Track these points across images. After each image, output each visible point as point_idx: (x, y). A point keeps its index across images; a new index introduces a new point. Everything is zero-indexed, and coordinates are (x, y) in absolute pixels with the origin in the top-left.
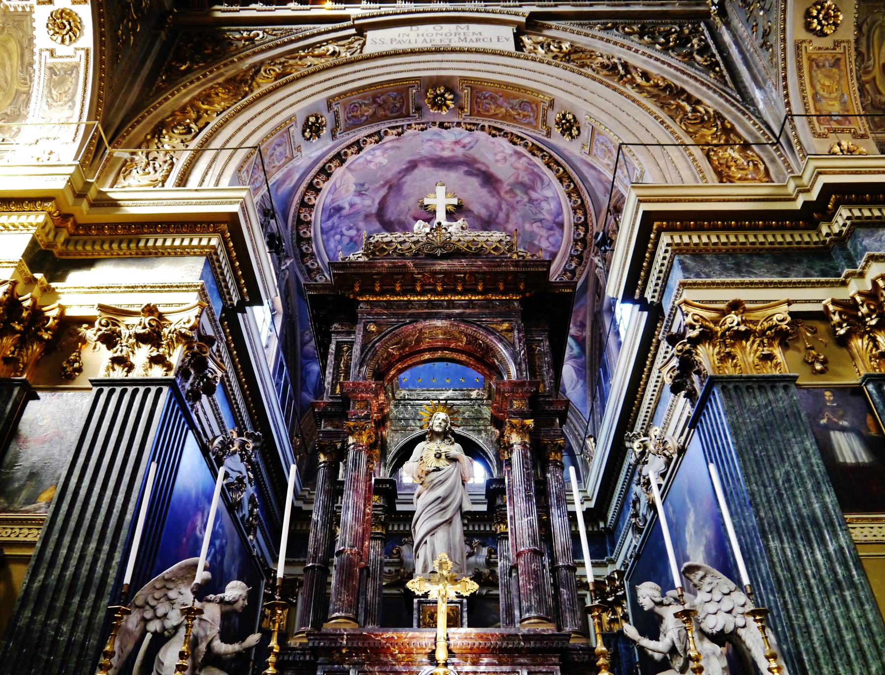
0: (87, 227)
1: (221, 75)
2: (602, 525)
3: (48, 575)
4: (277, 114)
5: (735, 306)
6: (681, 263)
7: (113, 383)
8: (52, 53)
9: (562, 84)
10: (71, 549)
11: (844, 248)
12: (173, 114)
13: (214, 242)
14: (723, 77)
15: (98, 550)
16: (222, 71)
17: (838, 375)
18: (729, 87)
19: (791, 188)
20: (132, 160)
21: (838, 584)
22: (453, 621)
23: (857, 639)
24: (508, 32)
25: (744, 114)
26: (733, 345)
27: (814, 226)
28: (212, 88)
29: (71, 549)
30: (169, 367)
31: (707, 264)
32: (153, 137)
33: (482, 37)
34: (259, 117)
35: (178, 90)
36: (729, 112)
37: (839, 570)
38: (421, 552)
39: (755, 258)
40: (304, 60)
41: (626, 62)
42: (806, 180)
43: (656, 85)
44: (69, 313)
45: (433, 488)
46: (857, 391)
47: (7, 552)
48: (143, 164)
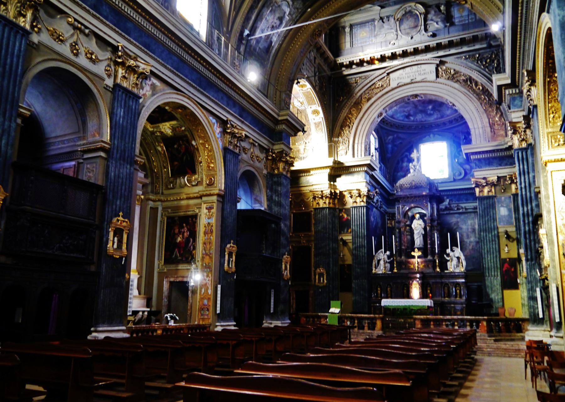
0: (337, 168)
1: (352, 102)
5: (484, 178)
7: (355, 207)
8: (314, 119)
17: (507, 192)
21: (492, 241)
24: (433, 67)
30: (364, 202)
31: (481, 163)
33: (425, 72)
37: (493, 238)
41: (471, 77)
43: (479, 88)
44: (341, 190)
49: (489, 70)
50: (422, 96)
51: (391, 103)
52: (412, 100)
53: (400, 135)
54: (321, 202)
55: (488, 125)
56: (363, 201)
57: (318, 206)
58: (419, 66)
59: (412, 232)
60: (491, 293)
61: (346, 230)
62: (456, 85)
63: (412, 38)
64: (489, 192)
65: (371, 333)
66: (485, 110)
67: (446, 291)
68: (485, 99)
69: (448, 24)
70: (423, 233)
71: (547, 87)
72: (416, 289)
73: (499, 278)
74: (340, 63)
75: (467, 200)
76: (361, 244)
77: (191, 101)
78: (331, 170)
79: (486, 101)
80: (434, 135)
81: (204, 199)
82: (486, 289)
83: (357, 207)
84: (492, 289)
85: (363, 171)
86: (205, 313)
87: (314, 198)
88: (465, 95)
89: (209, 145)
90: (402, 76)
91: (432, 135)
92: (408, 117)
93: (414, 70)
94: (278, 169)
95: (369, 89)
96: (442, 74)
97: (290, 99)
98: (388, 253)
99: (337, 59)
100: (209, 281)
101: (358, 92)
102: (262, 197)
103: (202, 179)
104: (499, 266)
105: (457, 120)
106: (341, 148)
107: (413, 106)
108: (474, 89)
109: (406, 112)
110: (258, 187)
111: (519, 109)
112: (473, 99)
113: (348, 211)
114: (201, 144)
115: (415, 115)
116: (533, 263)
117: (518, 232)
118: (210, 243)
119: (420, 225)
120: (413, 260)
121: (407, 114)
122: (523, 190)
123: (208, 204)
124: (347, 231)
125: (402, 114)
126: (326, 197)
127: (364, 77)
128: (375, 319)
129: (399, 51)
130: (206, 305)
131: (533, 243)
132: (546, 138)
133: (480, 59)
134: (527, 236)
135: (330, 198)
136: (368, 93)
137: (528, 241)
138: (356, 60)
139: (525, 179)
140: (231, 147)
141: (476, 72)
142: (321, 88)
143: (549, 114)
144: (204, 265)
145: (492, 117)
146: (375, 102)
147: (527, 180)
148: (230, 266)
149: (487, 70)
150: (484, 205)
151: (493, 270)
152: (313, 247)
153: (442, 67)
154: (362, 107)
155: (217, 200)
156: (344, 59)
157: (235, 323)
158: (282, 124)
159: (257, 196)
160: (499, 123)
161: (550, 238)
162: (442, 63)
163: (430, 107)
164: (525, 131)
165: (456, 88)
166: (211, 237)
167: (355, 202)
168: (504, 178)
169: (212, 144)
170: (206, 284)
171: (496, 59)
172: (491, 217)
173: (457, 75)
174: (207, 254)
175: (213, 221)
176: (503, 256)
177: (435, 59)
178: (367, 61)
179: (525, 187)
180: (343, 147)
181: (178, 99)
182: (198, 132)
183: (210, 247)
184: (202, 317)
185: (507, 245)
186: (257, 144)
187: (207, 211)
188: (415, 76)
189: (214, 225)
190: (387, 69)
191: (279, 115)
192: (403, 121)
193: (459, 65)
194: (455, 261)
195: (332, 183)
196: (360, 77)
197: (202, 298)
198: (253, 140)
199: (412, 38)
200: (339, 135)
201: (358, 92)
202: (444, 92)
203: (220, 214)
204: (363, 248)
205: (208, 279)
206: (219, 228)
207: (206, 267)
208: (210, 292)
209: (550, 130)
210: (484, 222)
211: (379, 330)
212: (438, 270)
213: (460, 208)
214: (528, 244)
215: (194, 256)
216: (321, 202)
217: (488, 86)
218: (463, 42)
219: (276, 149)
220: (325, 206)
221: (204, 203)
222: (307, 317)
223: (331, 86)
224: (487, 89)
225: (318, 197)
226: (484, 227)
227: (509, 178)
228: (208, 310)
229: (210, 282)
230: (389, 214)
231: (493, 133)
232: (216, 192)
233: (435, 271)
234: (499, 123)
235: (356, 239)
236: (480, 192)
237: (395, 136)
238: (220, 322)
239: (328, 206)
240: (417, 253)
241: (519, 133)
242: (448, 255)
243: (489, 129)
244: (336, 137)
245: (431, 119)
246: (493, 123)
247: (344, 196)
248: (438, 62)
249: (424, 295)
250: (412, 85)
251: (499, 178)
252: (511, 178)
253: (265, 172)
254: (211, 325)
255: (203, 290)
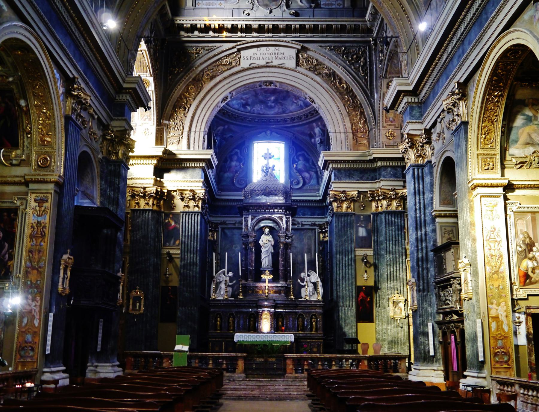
0: (166, 160)
1: (190, 77)
2: (324, 204)
3: (184, 262)
4: (214, 101)
5: (344, 192)
6: (334, 173)
7: (186, 213)
9: (310, 87)
10: (187, 256)
11: (379, 170)
12: (177, 100)
13: (204, 165)
14: (367, 82)
15: (194, 256)
16: (190, 75)
17: (367, 210)
18: (368, 89)
19: (367, 153)
20: (170, 123)
21: (349, 265)
22: (269, 282)
23: (349, 276)
24: (293, 52)
25: (369, 106)
26: (341, 203)
27: (373, 163)
28: (188, 86)
29: (187, 256)
31: (341, 174)
32: (174, 112)
34: (208, 103)
35: (177, 87)
36: (364, 104)
37: (350, 262)
38: (263, 261)
39: (355, 172)
40: (219, 67)
41: (335, 72)
42: (371, 152)
44: (169, 189)
45: (265, 248)
46: (369, 216)
47: (173, 256)
48: (174, 126)
49: (355, 68)
50: (277, 84)
51: (240, 87)
52: (264, 87)
53: (232, 127)
54: (142, 202)
55: (350, 131)
56: (197, 206)
57: (137, 207)
58: (277, 48)
59: (258, 248)
60: (345, 326)
61: (172, 242)
62: (318, 79)
63: (271, 12)
64: (348, 208)
65: (231, 376)
66: (348, 113)
67: (300, 324)
68: (349, 100)
69: (313, 5)
70: (273, 251)
71: (484, 104)
72: (266, 320)
73: (354, 308)
74: (178, 24)
75: (304, 214)
76: (192, 260)
77: (39, 43)
78: (158, 161)
79: (350, 102)
80: (272, 132)
81: (32, 186)
82: (339, 321)
83: (189, 213)
84: (345, 321)
85: (200, 167)
86: (27, 354)
87: (133, 196)
88: (328, 92)
89: (47, 110)
90: (256, 56)
91: (268, 132)
92: (244, 105)
93: (270, 52)
94: (117, 154)
95: (214, 64)
96: (303, 62)
97: (135, 61)
98: (231, 274)
99: (178, 18)
100: (35, 306)
101: (198, 66)
102: (95, 190)
103: (29, 157)
104: (354, 295)
105: (301, 118)
106: (172, 134)
107: (254, 93)
108: (337, 87)
109: (244, 100)
110: (90, 176)
111: (418, 121)
112: (336, 98)
113: (176, 217)
114: (36, 106)
115: (253, 105)
116: (425, 293)
117: (376, 257)
118: (39, 251)
119: (270, 241)
120: (263, 285)
121: (244, 102)
122: (418, 212)
123: (38, 195)
124: (174, 243)
125: (239, 101)
126: (151, 196)
127: (208, 48)
128: (236, 359)
129: (255, 24)
130: (30, 343)
131: (425, 272)
132: (476, 159)
133: (346, 53)
134: (420, 263)
135: (155, 198)
136: (212, 69)
137: (420, 269)
138: (200, 24)
139: (420, 199)
140: (74, 117)
141: (341, 67)
142: (155, 53)
143: (481, 134)
144: (29, 283)
145: (355, 122)
146: (220, 81)
147: (422, 201)
148: (65, 286)
149: (353, 67)
150: (342, 223)
151: (348, 298)
152: (128, 261)
153: (303, 54)
154: (202, 86)
155: (55, 191)
156: (185, 21)
157: (64, 368)
158: (126, 93)
159: (87, 188)
160: (362, 130)
161: (475, 269)
162: (304, 49)
163: (272, 98)
164: (422, 146)
165: (318, 81)
166: (43, 243)
167: (188, 206)
168: (364, 194)
169: (53, 109)
170: (30, 312)
171: (363, 56)
172: (348, 237)
173: (319, 67)
174: (33, 268)
175: (46, 220)
176: (359, 284)
177: (296, 43)
178: (201, 28)
179: (420, 208)
180: (174, 132)
181: (25, 36)
182: (34, 88)
183: (40, 258)
184: (22, 360)
185: (366, 271)
186: (96, 117)
187: (37, 204)
188: (271, 58)
189: (47, 225)
190: (238, 43)
191: (124, 81)
192: (238, 110)
193: (323, 56)
194: (311, 288)
195: (158, 179)
196: (203, 48)
197: (22, 332)
198: (94, 111)
199: (271, 12)
200: (170, 117)
201: (200, 65)
202: (305, 84)
203: (56, 213)
204: (195, 266)
205: (34, 304)
206: (54, 231)
207: (31, 287)
208: (36, 323)
209: (481, 151)
210: (340, 243)
211: (241, 373)
212: (292, 297)
213: (296, 223)
214: (421, 272)
215: (11, 270)
216: (142, 202)
217: (353, 86)
218: (328, 29)
219: (115, 127)
220: (147, 208)
221: (33, 193)
222: (136, 356)
223: (164, 51)
224: (352, 89)
225: (138, 195)
226: (340, 249)
227: (371, 194)
228: (33, 349)
229: (37, 310)
230: (212, 223)
231: (355, 140)
232: (56, 178)
233: (288, 298)
234: (362, 130)
235: (186, 254)
236: (338, 207)
237: (226, 127)
238: (50, 368)
239: (151, 208)
240: (267, 276)
241: (416, 148)
242: (303, 280)
243: (351, 136)
244: (166, 120)
245: (271, 113)
246: (356, 129)
247: (173, 197)
248: (299, 47)
249: (276, 328)
250: (268, 70)
251: (359, 192)
252: (372, 194)
253: (100, 156)
254: (37, 371)
255: (25, 321)
